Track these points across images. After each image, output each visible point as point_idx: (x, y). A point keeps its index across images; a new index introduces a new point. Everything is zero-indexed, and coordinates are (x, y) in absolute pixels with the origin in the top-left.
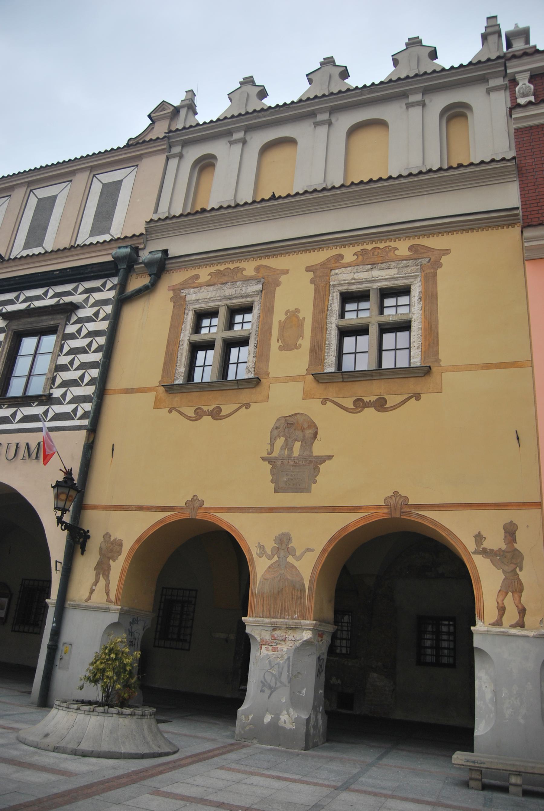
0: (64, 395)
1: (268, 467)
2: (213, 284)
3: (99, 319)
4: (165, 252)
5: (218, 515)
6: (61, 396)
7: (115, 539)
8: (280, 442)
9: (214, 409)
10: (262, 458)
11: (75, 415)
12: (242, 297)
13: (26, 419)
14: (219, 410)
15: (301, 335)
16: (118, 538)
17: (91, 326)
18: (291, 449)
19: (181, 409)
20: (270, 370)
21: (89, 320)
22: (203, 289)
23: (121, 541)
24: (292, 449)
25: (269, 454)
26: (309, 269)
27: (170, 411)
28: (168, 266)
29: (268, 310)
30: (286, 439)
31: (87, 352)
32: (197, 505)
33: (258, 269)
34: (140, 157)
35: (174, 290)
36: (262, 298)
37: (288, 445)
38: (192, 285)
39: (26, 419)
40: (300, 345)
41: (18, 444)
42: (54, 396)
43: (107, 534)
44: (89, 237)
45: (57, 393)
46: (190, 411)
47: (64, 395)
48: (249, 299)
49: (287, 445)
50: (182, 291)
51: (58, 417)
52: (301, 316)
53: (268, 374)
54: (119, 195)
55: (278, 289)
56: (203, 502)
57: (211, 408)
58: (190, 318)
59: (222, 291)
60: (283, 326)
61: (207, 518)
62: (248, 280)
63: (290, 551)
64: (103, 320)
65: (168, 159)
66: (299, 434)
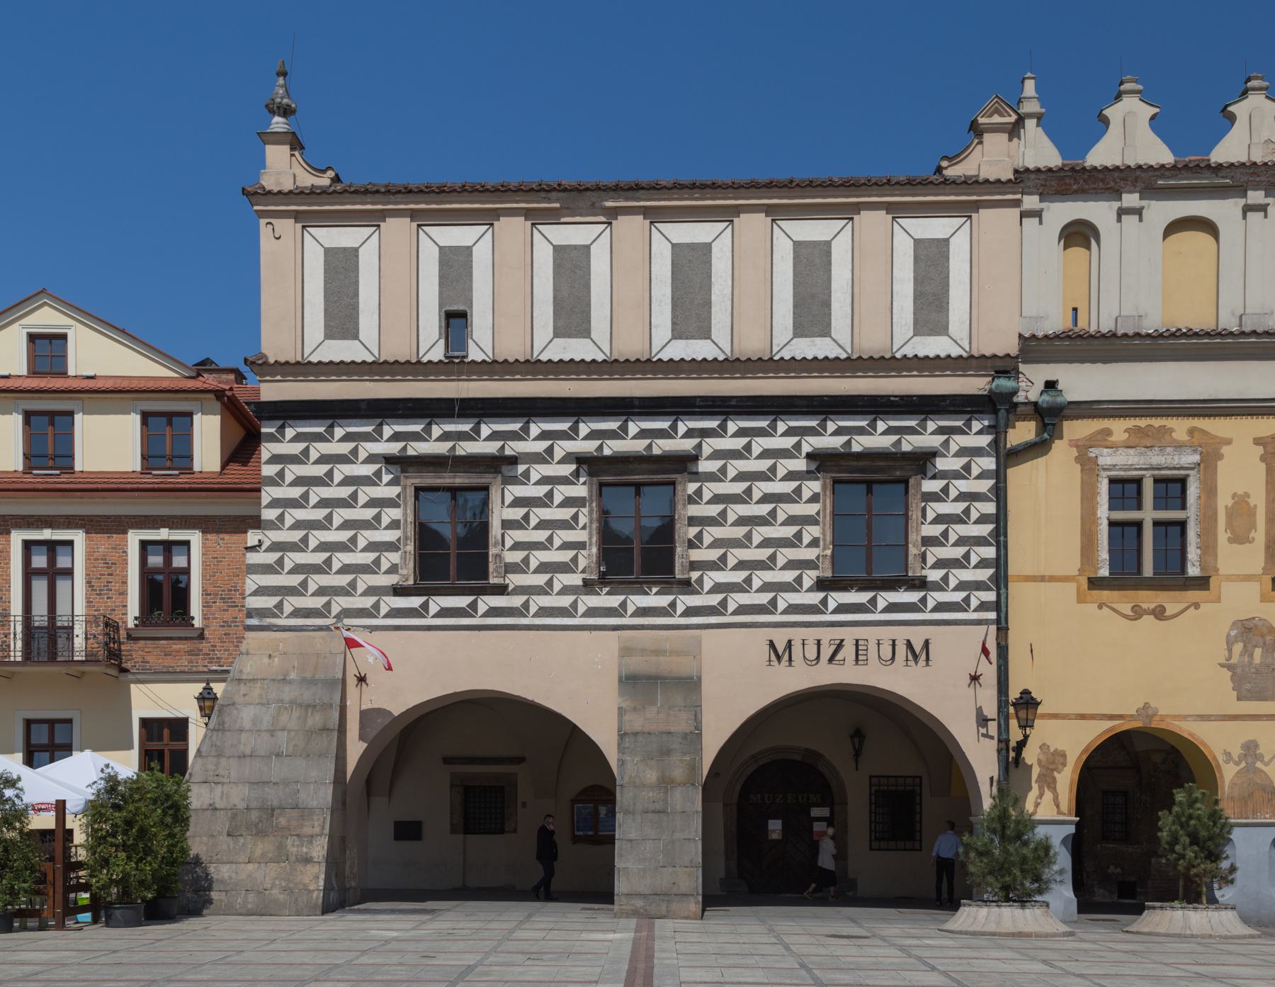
0: (945, 579)
1: (1227, 674)
2: (1133, 445)
3: (973, 476)
4: (1051, 385)
5: (1176, 723)
6: (941, 579)
7: (1056, 750)
8: (1238, 648)
9: (1156, 608)
10: (1220, 664)
11: (969, 606)
12: (1175, 468)
13: (892, 608)
14: (1163, 609)
15: (1253, 526)
16: (1060, 749)
17: (963, 486)
18: (1251, 655)
19: (1114, 606)
20: (1219, 565)
21: (956, 475)
22: (1121, 451)
23: (1064, 751)
24: (1252, 655)
25: (1227, 660)
26: (1257, 441)
27: (1100, 607)
28: (1066, 412)
29: (1210, 490)
30: (1245, 646)
31: (965, 523)
32: (1150, 712)
33: (1191, 432)
34: (976, 206)
35: (1077, 446)
36: (1201, 472)
37: (1247, 652)
38: (1103, 443)
39: (892, 608)
40: (1253, 539)
41: (894, 641)
42: (929, 579)
43: (1044, 744)
44: (914, 335)
45: (934, 575)
46: (1126, 609)
47: (945, 579)
48: (1183, 472)
49: (1246, 651)
50: (1090, 450)
51: (940, 607)
52: (1252, 502)
53: (1217, 570)
54: (948, 268)
55: (1219, 463)
56: (1157, 710)
57: (1152, 606)
58: (1104, 487)
59: (1147, 458)
60: (1231, 513)
61: (1163, 726)
62: (1179, 446)
63: (1260, 758)
64: (979, 477)
65: (1024, 215)
66: (1261, 641)
